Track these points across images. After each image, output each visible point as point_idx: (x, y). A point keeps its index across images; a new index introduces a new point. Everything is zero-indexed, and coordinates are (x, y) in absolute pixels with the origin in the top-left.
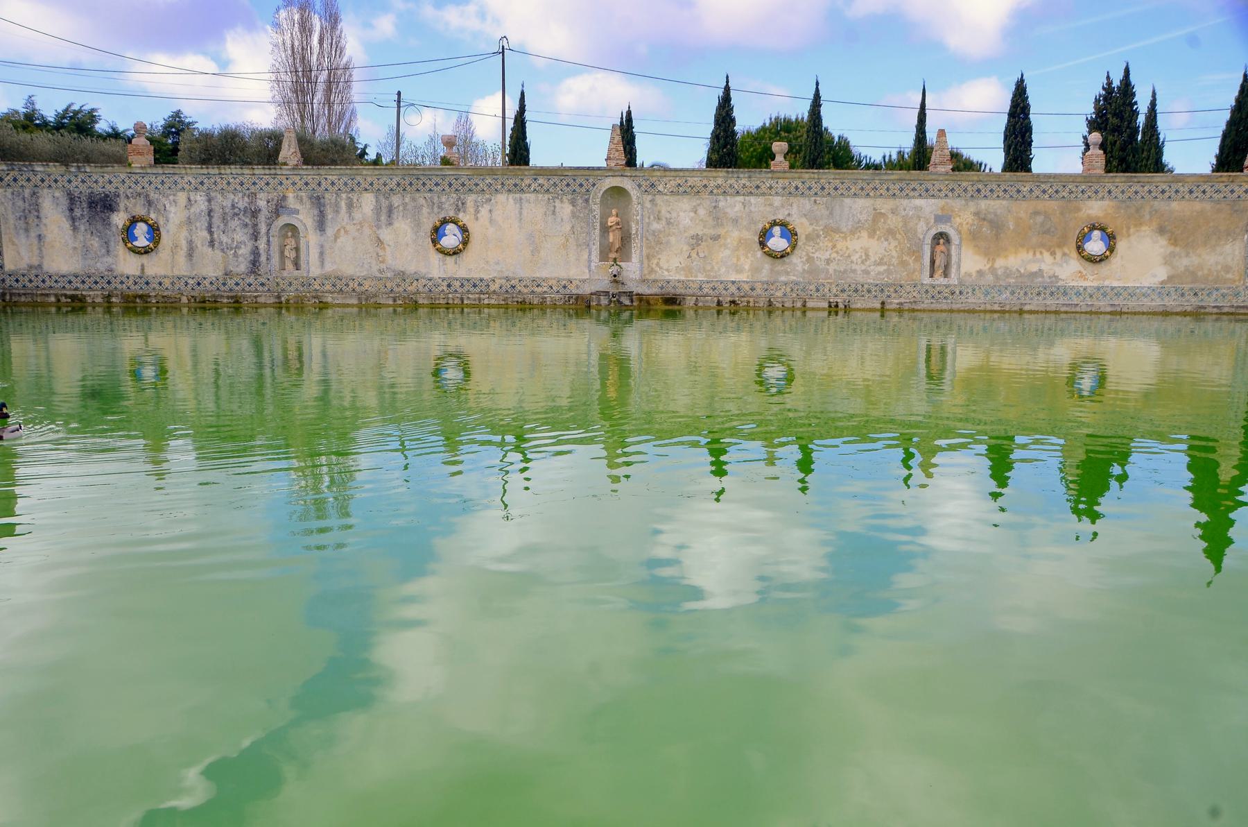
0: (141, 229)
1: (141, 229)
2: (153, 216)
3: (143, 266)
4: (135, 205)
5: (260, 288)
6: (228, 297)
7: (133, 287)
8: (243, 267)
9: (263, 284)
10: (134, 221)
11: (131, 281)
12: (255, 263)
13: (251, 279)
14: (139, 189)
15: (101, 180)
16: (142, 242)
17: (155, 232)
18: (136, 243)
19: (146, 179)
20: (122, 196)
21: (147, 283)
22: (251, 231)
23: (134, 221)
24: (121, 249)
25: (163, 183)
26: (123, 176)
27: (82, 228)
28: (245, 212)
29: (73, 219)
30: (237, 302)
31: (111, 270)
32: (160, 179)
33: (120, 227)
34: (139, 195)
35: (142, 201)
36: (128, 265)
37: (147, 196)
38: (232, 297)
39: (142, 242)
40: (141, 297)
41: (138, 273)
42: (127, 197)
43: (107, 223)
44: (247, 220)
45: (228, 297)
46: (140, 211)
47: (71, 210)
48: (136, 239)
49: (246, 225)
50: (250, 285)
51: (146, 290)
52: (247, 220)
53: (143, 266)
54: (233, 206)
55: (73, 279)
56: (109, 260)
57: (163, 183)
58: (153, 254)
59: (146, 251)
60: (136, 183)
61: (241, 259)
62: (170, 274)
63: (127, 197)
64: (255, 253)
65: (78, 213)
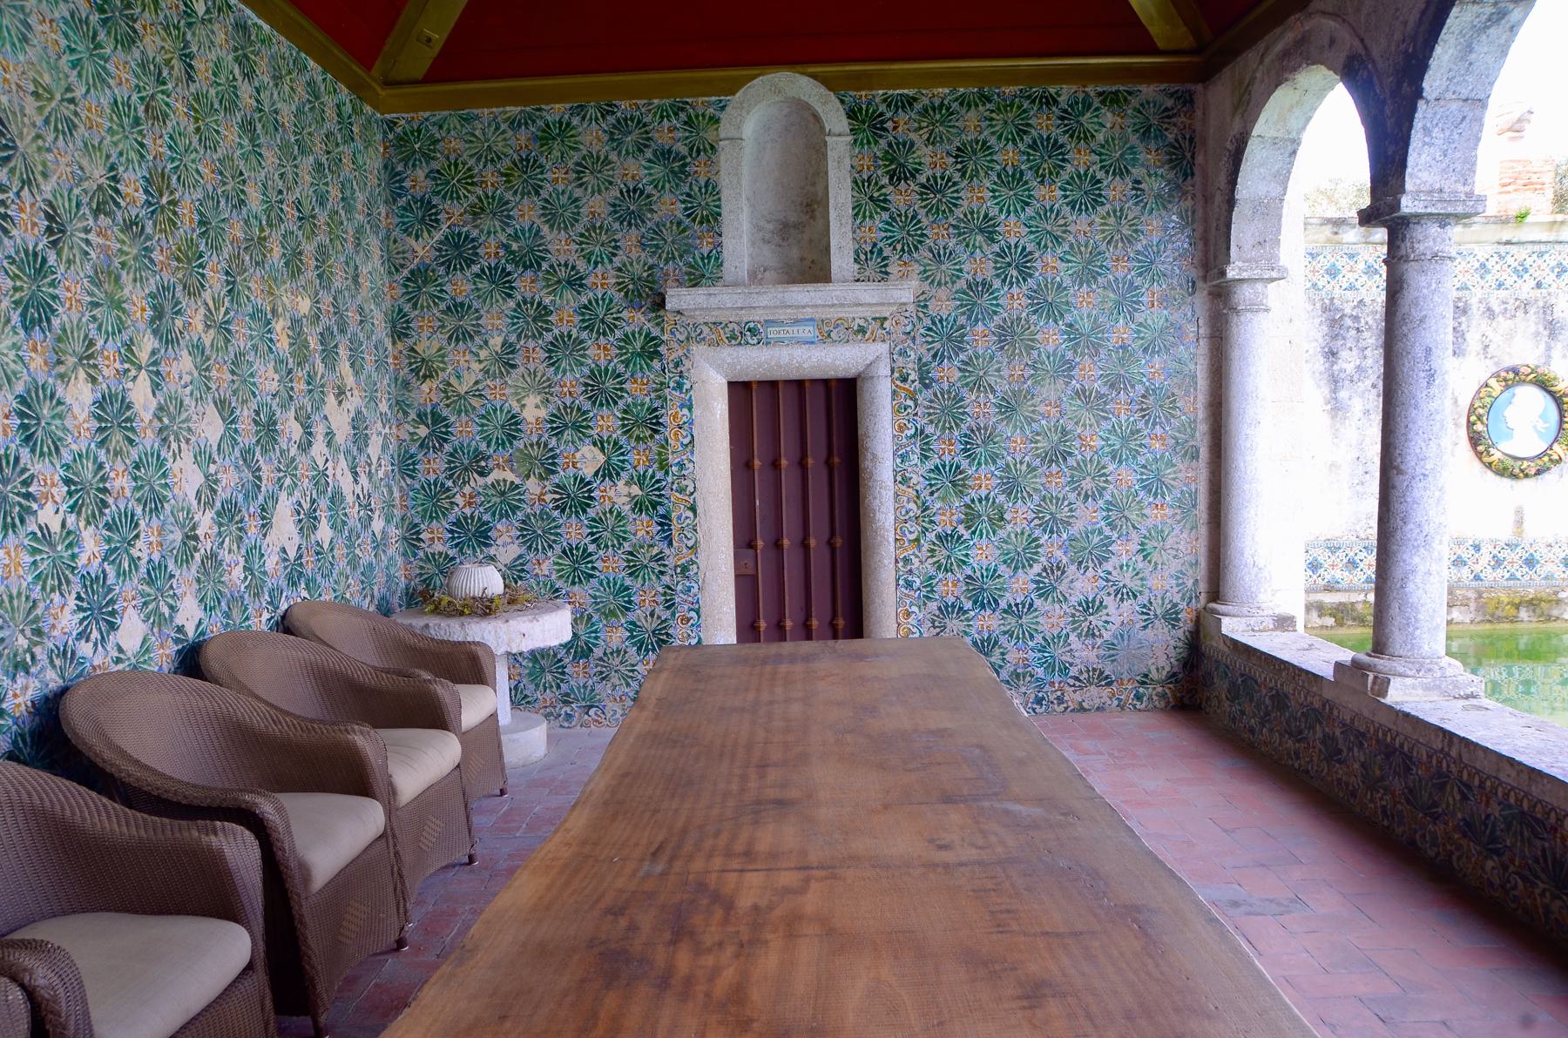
3: (1519, 512)
7: (1490, 575)
11: (1485, 558)
14: (1526, 289)
19: (1551, 260)
20: (1476, 309)
21: (1530, 562)
26: (1482, 252)
27: (1357, 406)
29: (1335, 382)
34: (1525, 306)
35: (1530, 323)
37: (1548, 308)
40: (1533, 604)
41: (1505, 533)
42: (1490, 313)
47: (1332, 354)
51: (1531, 583)
53: (1519, 512)
55: (1323, 556)
60: (1521, 271)
63: (1490, 313)
65: (1348, 361)
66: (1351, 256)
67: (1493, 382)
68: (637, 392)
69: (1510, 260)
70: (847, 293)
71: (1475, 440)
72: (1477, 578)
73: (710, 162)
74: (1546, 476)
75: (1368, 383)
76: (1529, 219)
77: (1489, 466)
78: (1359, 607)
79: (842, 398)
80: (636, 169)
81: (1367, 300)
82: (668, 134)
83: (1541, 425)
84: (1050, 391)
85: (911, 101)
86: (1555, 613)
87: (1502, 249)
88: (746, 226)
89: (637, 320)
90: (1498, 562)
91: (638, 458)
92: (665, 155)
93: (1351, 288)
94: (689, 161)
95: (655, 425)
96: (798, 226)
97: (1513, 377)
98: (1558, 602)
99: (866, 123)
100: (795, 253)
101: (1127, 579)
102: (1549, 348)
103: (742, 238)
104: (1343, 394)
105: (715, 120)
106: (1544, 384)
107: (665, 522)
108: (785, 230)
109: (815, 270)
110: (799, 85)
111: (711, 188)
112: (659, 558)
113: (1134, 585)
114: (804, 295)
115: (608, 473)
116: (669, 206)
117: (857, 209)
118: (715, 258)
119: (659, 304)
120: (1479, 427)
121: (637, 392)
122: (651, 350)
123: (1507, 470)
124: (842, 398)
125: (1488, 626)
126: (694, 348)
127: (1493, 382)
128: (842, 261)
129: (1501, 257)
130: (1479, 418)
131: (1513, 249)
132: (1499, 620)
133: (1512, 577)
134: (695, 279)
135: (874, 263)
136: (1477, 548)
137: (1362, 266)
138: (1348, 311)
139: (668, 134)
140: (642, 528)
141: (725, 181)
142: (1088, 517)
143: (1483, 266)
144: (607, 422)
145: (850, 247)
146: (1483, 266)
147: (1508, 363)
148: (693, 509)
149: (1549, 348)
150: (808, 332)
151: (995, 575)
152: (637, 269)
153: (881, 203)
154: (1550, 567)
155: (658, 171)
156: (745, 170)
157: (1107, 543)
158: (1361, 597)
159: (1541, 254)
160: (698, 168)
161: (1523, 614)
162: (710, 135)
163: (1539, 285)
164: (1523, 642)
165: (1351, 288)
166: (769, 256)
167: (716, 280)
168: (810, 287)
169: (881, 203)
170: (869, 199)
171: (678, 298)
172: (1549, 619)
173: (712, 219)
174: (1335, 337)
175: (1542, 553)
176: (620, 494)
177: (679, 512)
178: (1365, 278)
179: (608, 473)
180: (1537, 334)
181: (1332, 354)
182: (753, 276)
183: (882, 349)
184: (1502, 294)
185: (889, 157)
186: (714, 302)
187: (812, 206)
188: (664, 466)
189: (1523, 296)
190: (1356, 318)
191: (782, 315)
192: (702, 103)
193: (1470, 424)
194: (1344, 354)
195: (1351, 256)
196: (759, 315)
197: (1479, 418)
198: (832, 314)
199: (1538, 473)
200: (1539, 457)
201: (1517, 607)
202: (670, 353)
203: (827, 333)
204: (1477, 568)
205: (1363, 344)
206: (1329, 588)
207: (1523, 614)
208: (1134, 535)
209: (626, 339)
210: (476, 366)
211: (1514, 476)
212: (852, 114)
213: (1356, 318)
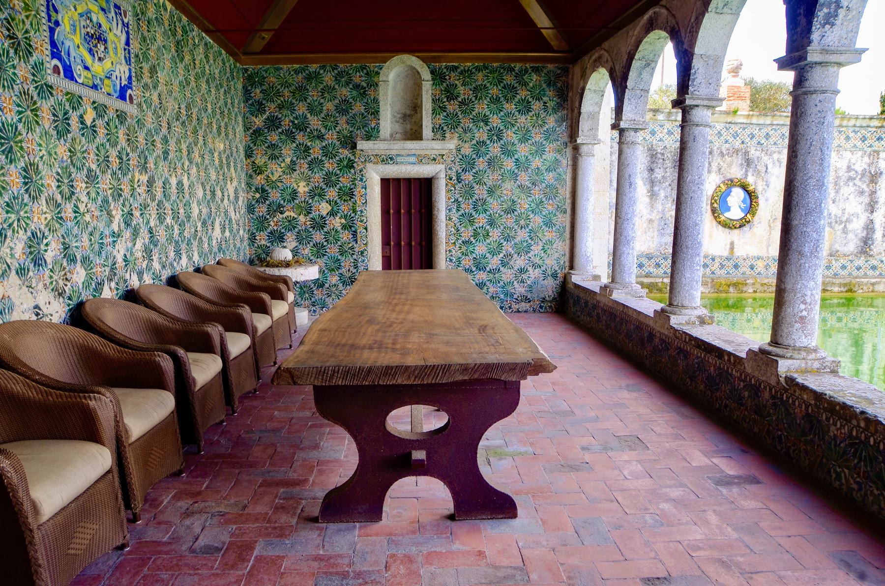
0: (737, 197)
2: (751, 179)
3: (732, 244)
4: (730, 165)
5: (870, 273)
6: (840, 285)
7: (718, 272)
8: (852, 246)
9: (874, 268)
11: (717, 264)
12: (866, 242)
13: (861, 262)
14: (737, 144)
18: (727, 215)
19: (748, 131)
21: (736, 266)
22: (867, 200)
25: (767, 136)
26: (719, 127)
27: (662, 194)
28: (863, 175)
30: (850, 290)
32: (764, 131)
34: (737, 151)
35: (739, 160)
37: (746, 153)
38: (845, 285)
39: (735, 213)
40: (735, 285)
41: (726, 254)
42: (722, 154)
44: (864, 186)
45: (840, 285)
46: (736, 172)
47: (651, 170)
48: (728, 209)
49: (862, 193)
50: (859, 268)
52: (864, 186)
53: (732, 244)
54: (849, 169)
55: (645, 261)
57: (767, 136)
59: (742, 224)
61: (851, 236)
62: (764, 255)
63: (722, 154)
64: (869, 227)
65: (659, 174)
66: (661, 126)
67: (722, 185)
68: (345, 181)
69: (731, 131)
70: (429, 145)
71: (714, 211)
72: (713, 273)
73: (376, 90)
74: (744, 228)
75: (667, 184)
76: (739, 113)
77: (720, 223)
78: (660, 284)
79: (426, 186)
80: (345, 92)
81: (668, 146)
82: (358, 78)
83: (743, 206)
84: (508, 185)
85: (456, 68)
86: (745, 289)
87: (728, 125)
88: (389, 116)
89: (345, 153)
90: (722, 266)
91: (344, 208)
92: (357, 87)
93: (661, 140)
94: (367, 91)
95: (351, 195)
96: (410, 116)
97: (731, 184)
98: (746, 284)
99: (438, 77)
100: (408, 127)
101: (537, 260)
102: (747, 171)
103: (387, 121)
104: (656, 188)
105: (378, 73)
106: (744, 187)
107: (355, 234)
108: (405, 117)
109: (415, 134)
110: (413, 61)
111: (376, 101)
112: (352, 248)
113: (540, 262)
114: (412, 146)
115: (332, 213)
116: (359, 107)
117: (434, 110)
118: (377, 129)
119: (354, 146)
120: (715, 205)
121: (345, 181)
122: (350, 165)
123: (728, 225)
124: (426, 186)
125: (716, 295)
126: (367, 165)
127: (722, 185)
128: (427, 132)
130: (716, 201)
131: (733, 126)
132: (721, 292)
133: (728, 273)
134: (368, 137)
135: (440, 132)
136: (713, 260)
137: (666, 130)
138: (659, 151)
139: (358, 78)
140: (345, 236)
141: (381, 98)
142: (522, 235)
143: (719, 133)
144: (332, 194)
145: (431, 126)
146: (719, 133)
147: (729, 176)
148: (366, 229)
149: (747, 171)
150: (413, 159)
151: (485, 257)
152: (345, 132)
153: (443, 109)
154: (744, 269)
155: (355, 93)
156: (390, 93)
157: (529, 246)
158: (661, 280)
159: (744, 129)
160: (371, 92)
161: (731, 289)
162: (376, 79)
163: (743, 143)
164: (730, 302)
165: (661, 140)
166: (398, 127)
167: (377, 138)
168: (414, 142)
169: (443, 109)
170: (439, 107)
171: (362, 145)
172: (742, 292)
173: (376, 113)
174: (653, 163)
175: (741, 262)
176: (337, 222)
177: (360, 230)
179: (332, 213)
180: (742, 164)
181: (651, 170)
182: (391, 135)
183: (442, 167)
184: (727, 145)
185: (447, 90)
186: (376, 147)
187: (415, 108)
188: (355, 211)
189: (736, 147)
190: (663, 154)
191: (402, 152)
192: (373, 66)
193: (712, 204)
194: (657, 170)
195: (661, 126)
196: (394, 152)
197: (716, 201)
198: (423, 153)
199: (740, 227)
200: (741, 219)
201: (729, 286)
202: (358, 166)
203: (421, 160)
204: (713, 269)
205: (665, 166)
206: (647, 276)
207: (731, 289)
208: (540, 243)
209: (341, 160)
210: (280, 170)
211: (730, 228)
212: (432, 73)
213: (663, 154)
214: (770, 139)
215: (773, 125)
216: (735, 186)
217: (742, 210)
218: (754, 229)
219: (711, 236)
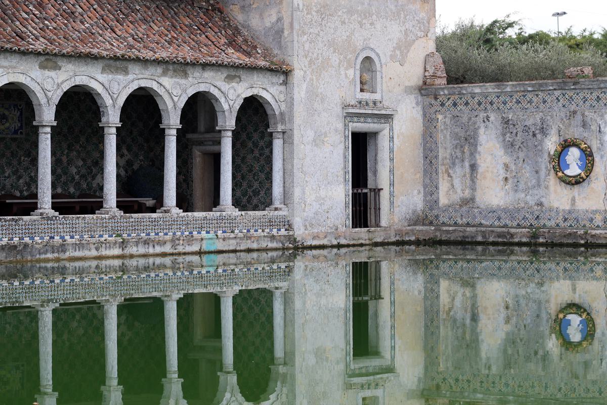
0: (574, 154)
1: (574, 154)
7: (562, 224)
10: (566, 145)
15: (535, 99)
16: (574, 170)
17: (588, 156)
23: (566, 145)
24: (552, 181)
31: (540, 204)
33: (552, 153)
36: (559, 198)
39: (574, 170)
41: (568, 207)
43: (538, 149)
46: (575, 132)
48: (568, 166)
56: (541, 192)
58: (585, 184)
59: (577, 181)
83: (579, 163)
90: (566, 220)
101: (262, 200)
107: (188, 184)
113: (264, 201)
129: (564, 95)
142: (256, 185)
143: (557, 99)
148: (192, 182)
151: (240, 198)
157: (259, 191)
178: (516, 105)
188: (188, 172)
208: (264, 190)
210: (159, 149)
214: (600, 101)
215: (602, 88)
216: (569, 146)
217: (580, 167)
218: (592, 185)
219: (555, 192)
